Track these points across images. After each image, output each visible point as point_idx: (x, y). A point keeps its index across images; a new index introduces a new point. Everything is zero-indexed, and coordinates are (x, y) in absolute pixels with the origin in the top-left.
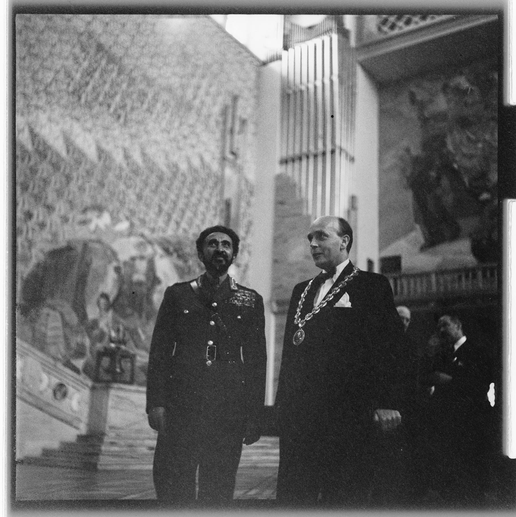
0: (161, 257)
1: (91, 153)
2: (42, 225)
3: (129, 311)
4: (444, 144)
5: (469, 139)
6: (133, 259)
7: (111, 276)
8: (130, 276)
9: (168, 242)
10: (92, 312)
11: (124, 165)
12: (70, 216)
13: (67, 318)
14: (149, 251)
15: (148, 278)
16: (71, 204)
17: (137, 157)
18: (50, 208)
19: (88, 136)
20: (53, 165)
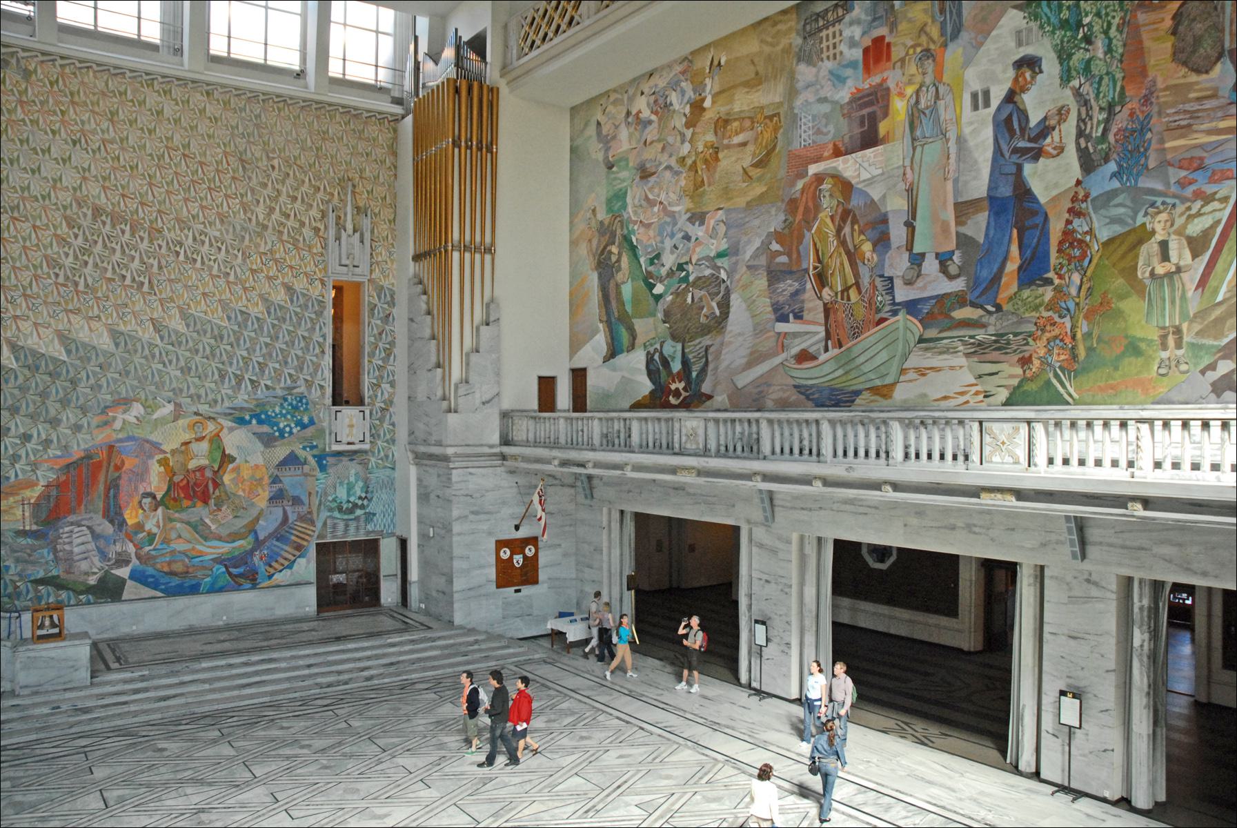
0: (231, 430)
1: (104, 341)
2: (47, 443)
3: (185, 503)
4: (624, 207)
5: (647, 198)
6: (186, 444)
7: (156, 470)
8: (184, 465)
9: (242, 409)
10: (131, 517)
11: (158, 341)
12: (84, 422)
13: (98, 529)
14: (211, 427)
15: (214, 461)
16: (84, 410)
17: (177, 324)
18: (54, 422)
19: (94, 324)
20: (50, 374)
